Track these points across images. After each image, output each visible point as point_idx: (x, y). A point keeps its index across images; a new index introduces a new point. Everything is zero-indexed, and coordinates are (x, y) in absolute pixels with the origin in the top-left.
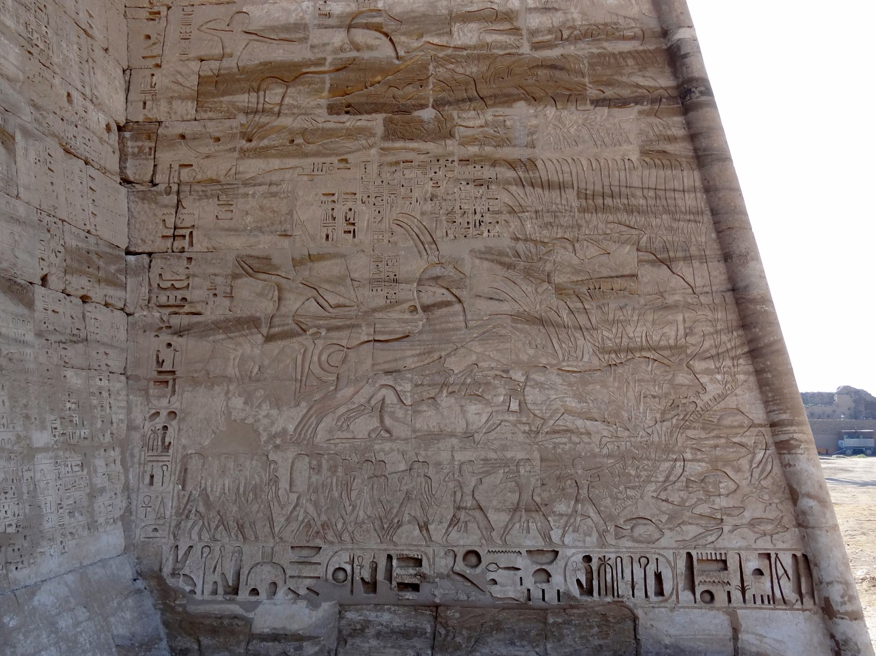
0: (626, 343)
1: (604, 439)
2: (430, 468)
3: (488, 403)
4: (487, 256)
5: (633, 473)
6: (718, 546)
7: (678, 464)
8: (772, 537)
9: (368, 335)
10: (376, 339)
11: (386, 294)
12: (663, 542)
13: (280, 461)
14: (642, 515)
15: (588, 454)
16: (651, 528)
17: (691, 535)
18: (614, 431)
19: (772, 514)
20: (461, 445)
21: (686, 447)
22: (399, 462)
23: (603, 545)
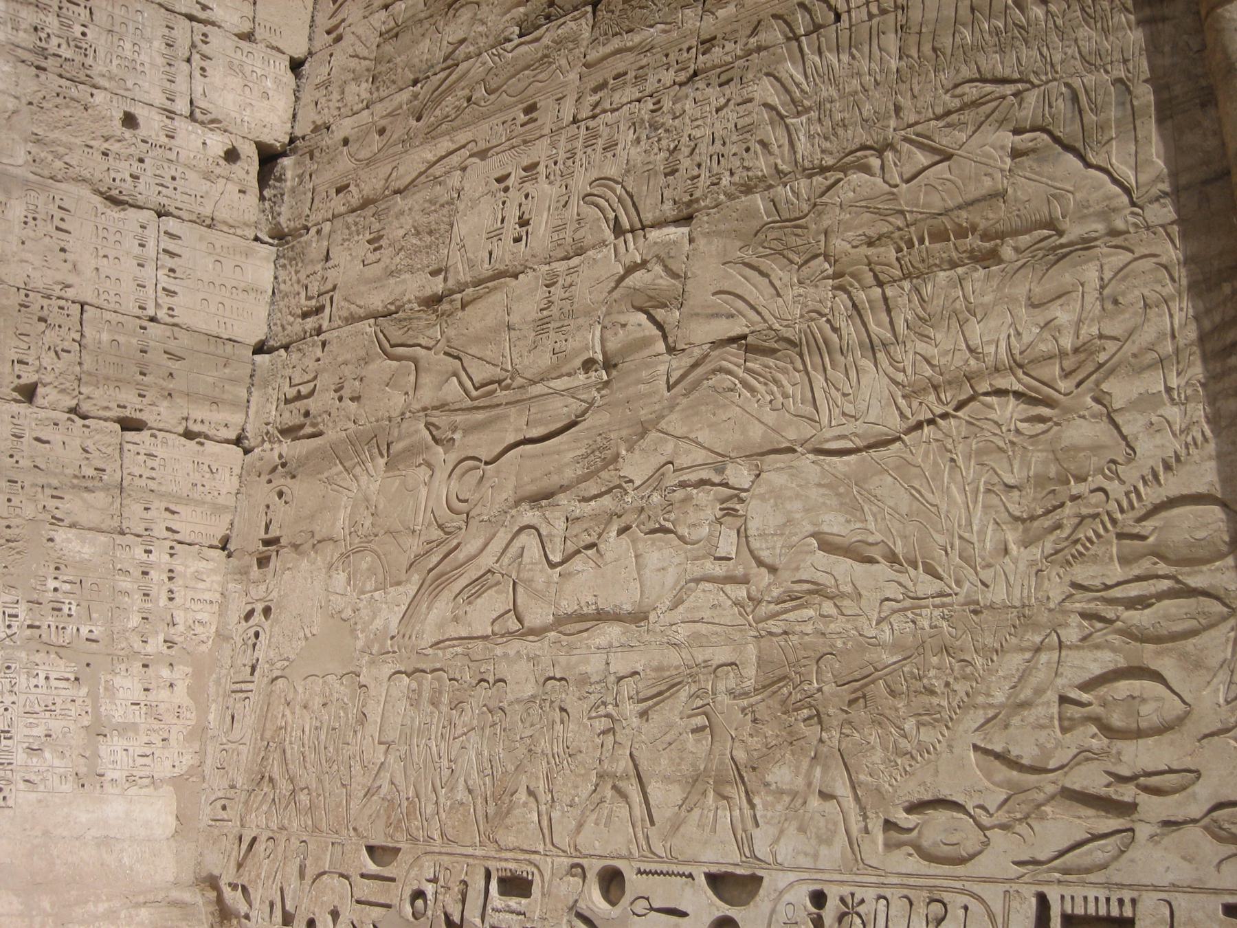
5: (938, 685)
12: (980, 866)
13: (372, 685)
14: (945, 793)
15: (849, 646)
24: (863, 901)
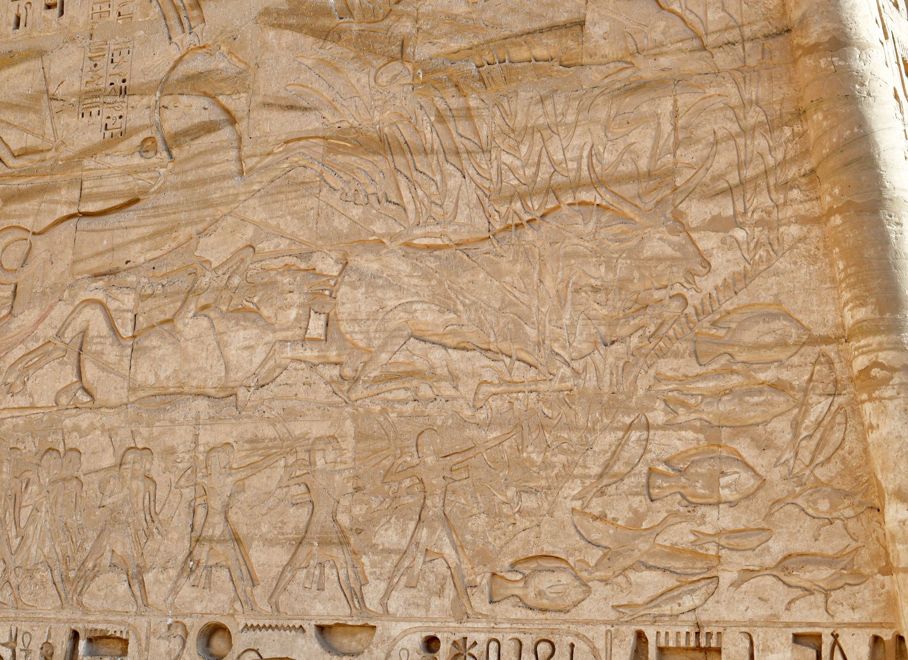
0: (547, 176)
1: (485, 388)
2: (156, 459)
3: (269, 326)
4: (292, 21)
5: (537, 458)
6: (704, 617)
7: (635, 435)
8: (827, 596)
9: (71, 204)
10: (83, 210)
11: (105, 121)
14: (548, 549)
16: (565, 578)
17: (650, 592)
18: (504, 370)
19: (830, 546)
20: (212, 412)
21: (654, 398)
22: (103, 450)
23: (463, 614)
24: (475, 643)
